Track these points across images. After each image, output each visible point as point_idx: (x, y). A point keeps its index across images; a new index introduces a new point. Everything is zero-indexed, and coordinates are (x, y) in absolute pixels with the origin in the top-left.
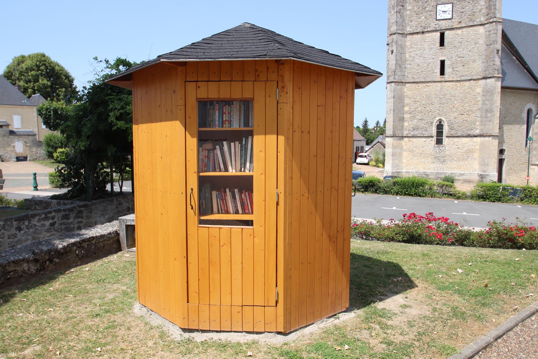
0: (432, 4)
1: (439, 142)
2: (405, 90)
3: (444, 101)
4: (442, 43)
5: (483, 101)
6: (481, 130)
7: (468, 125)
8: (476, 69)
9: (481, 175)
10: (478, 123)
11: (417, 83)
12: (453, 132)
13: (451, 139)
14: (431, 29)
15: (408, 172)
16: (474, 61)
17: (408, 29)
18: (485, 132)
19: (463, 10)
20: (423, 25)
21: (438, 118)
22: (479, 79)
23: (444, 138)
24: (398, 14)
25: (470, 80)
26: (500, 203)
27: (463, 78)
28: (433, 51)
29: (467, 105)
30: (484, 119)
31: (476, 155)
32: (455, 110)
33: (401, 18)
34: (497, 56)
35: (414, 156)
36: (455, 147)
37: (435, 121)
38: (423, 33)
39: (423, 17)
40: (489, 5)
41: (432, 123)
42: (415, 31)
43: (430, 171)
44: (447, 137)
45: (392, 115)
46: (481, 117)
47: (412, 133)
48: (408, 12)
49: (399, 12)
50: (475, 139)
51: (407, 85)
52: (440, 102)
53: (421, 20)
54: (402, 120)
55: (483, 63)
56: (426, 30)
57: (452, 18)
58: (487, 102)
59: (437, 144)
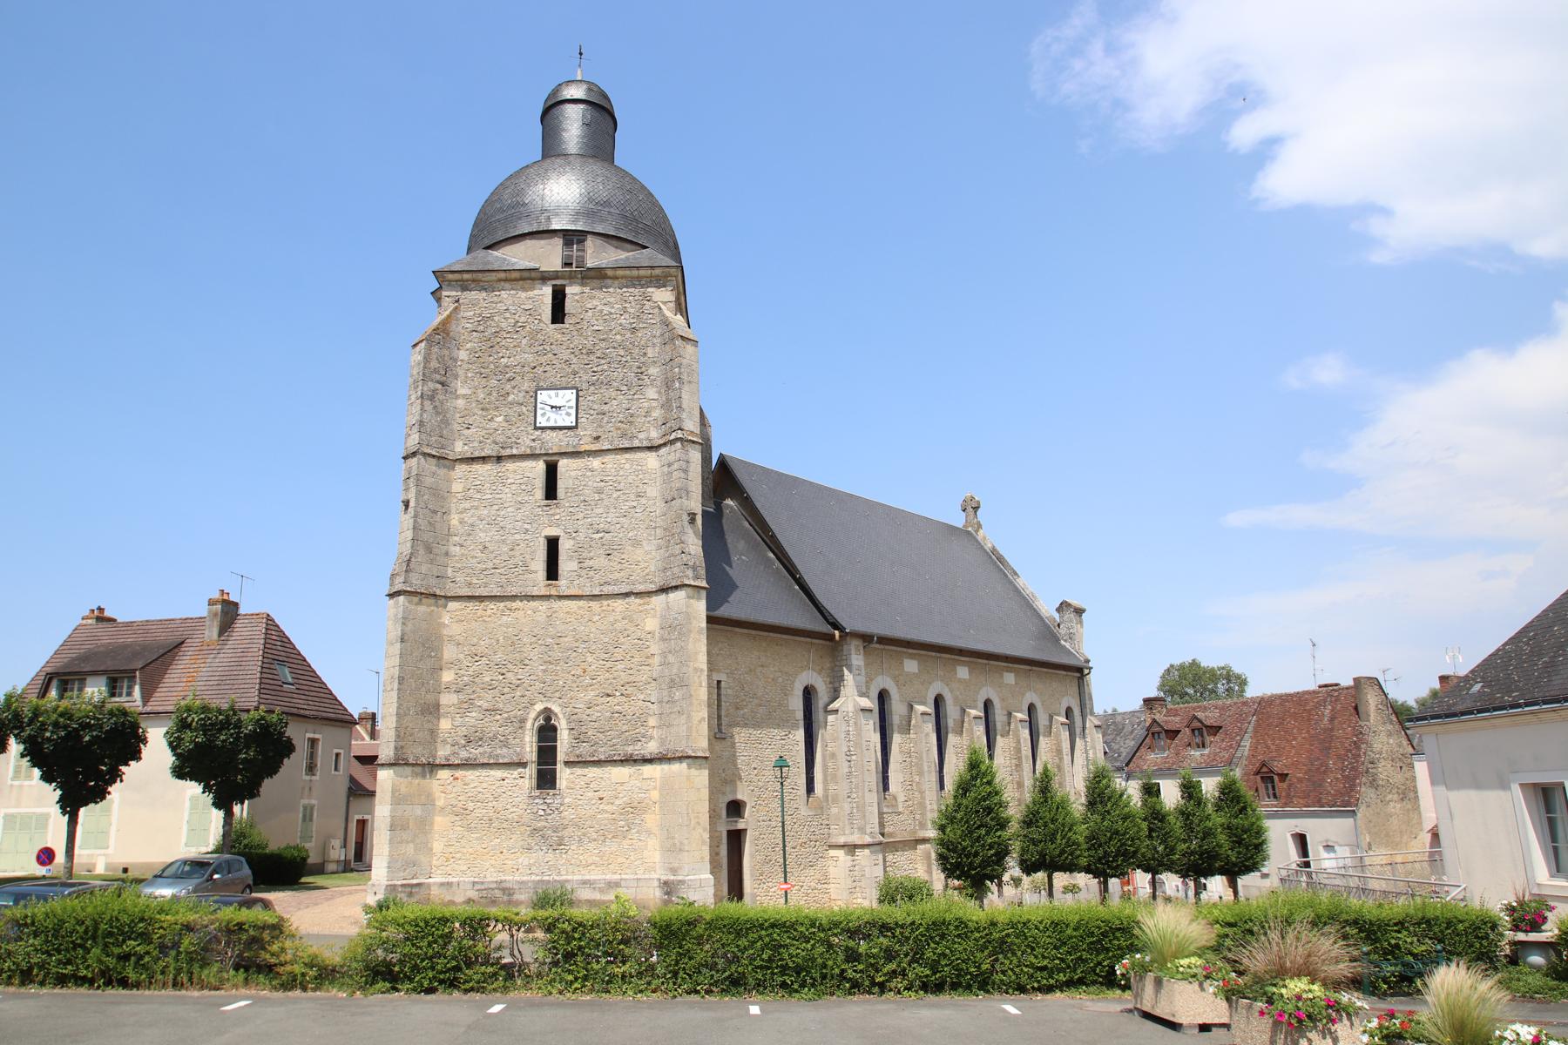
0: (526, 386)
1: (546, 780)
2: (446, 619)
3: (556, 654)
4: (551, 491)
5: (664, 654)
6: (662, 742)
7: (625, 728)
8: (642, 565)
9: (666, 883)
10: (652, 722)
11: (481, 598)
12: (584, 750)
13: (579, 771)
14: (522, 450)
15: (449, 884)
16: (637, 543)
17: (459, 448)
18: (671, 747)
19: (606, 408)
20: (501, 439)
21: (539, 707)
22: (649, 593)
23: (559, 767)
24: (427, 403)
25: (627, 595)
26: (456, 994)
27: (607, 589)
28: (526, 509)
29: (620, 666)
32: (588, 681)
33: (438, 413)
34: (689, 530)
35: (469, 829)
36: (590, 794)
37: (533, 715)
38: (499, 459)
39: (500, 419)
40: (669, 400)
41: (523, 721)
42: (477, 454)
43: (517, 878)
44: (567, 763)
45: (394, 694)
47: (464, 754)
48: (460, 403)
49: (432, 398)
50: (648, 770)
51: (452, 605)
52: (546, 658)
53: (495, 425)
54: (432, 710)
56: (508, 452)
57: (576, 427)
58: (671, 658)
59: (539, 787)
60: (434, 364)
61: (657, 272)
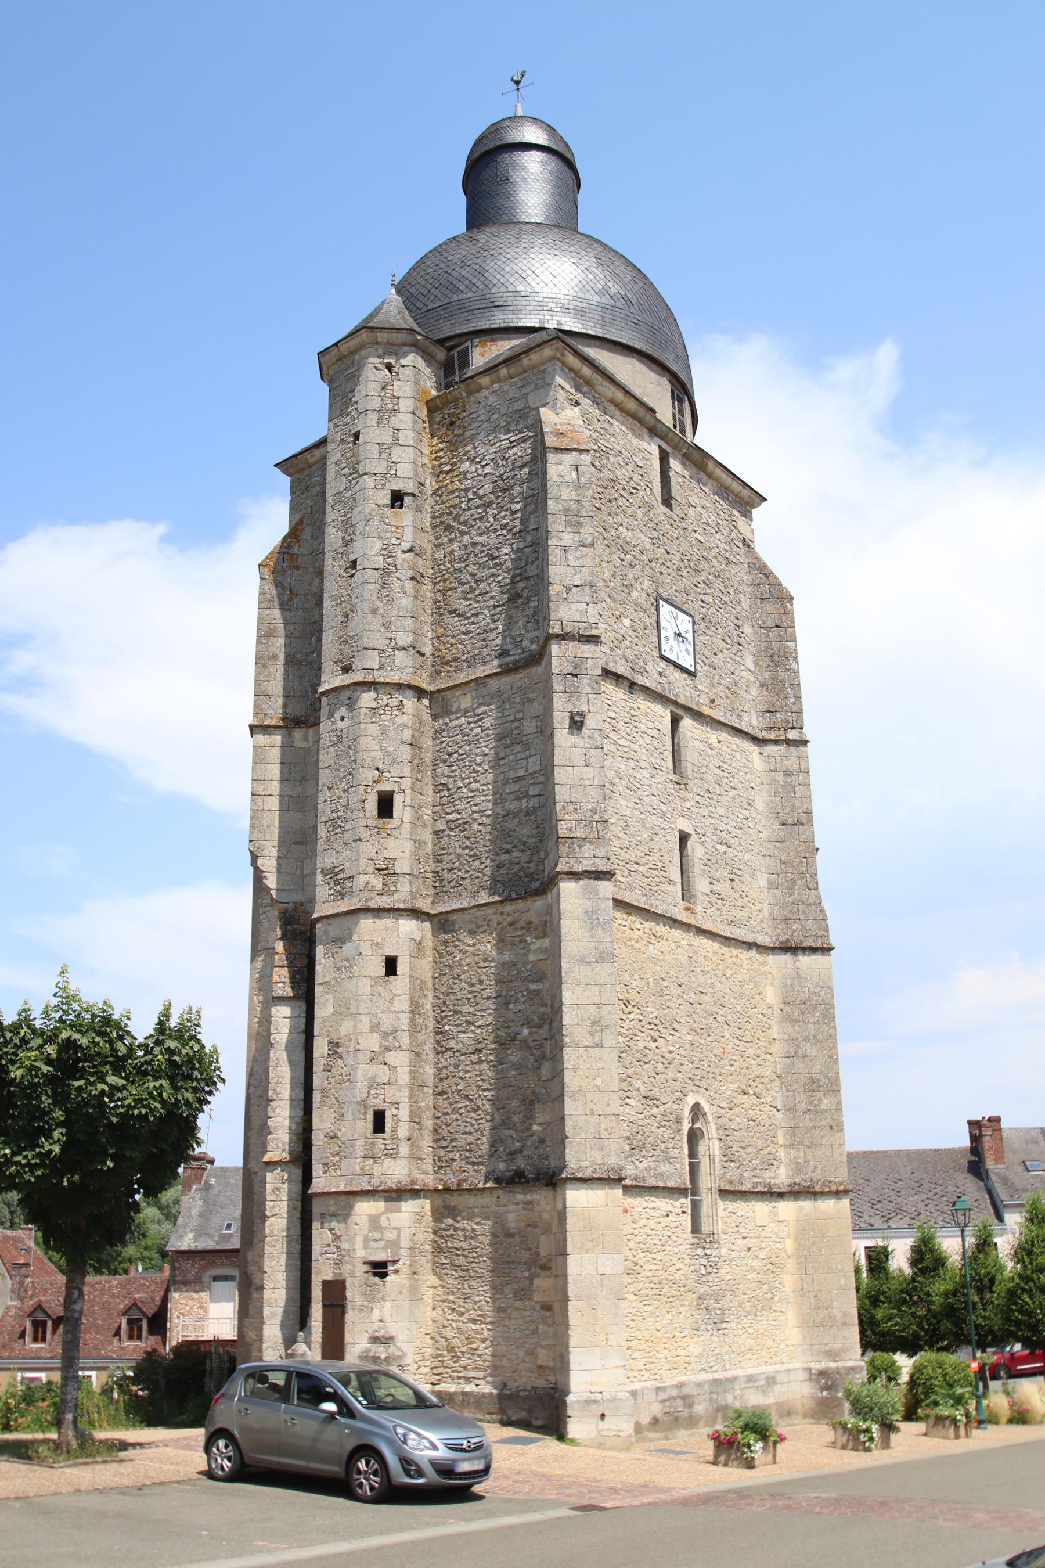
5: (792, 1041)
6: (798, 1168)
9: (822, 1373)
10: (781, 1140)
12: (733, 1173)
18: (817, 1175)
30: (807, 1121)
31: (788, 1281)
46: (792, 1110)
55: (772, 886)
58: (810, 1049)
61: (746, 493)
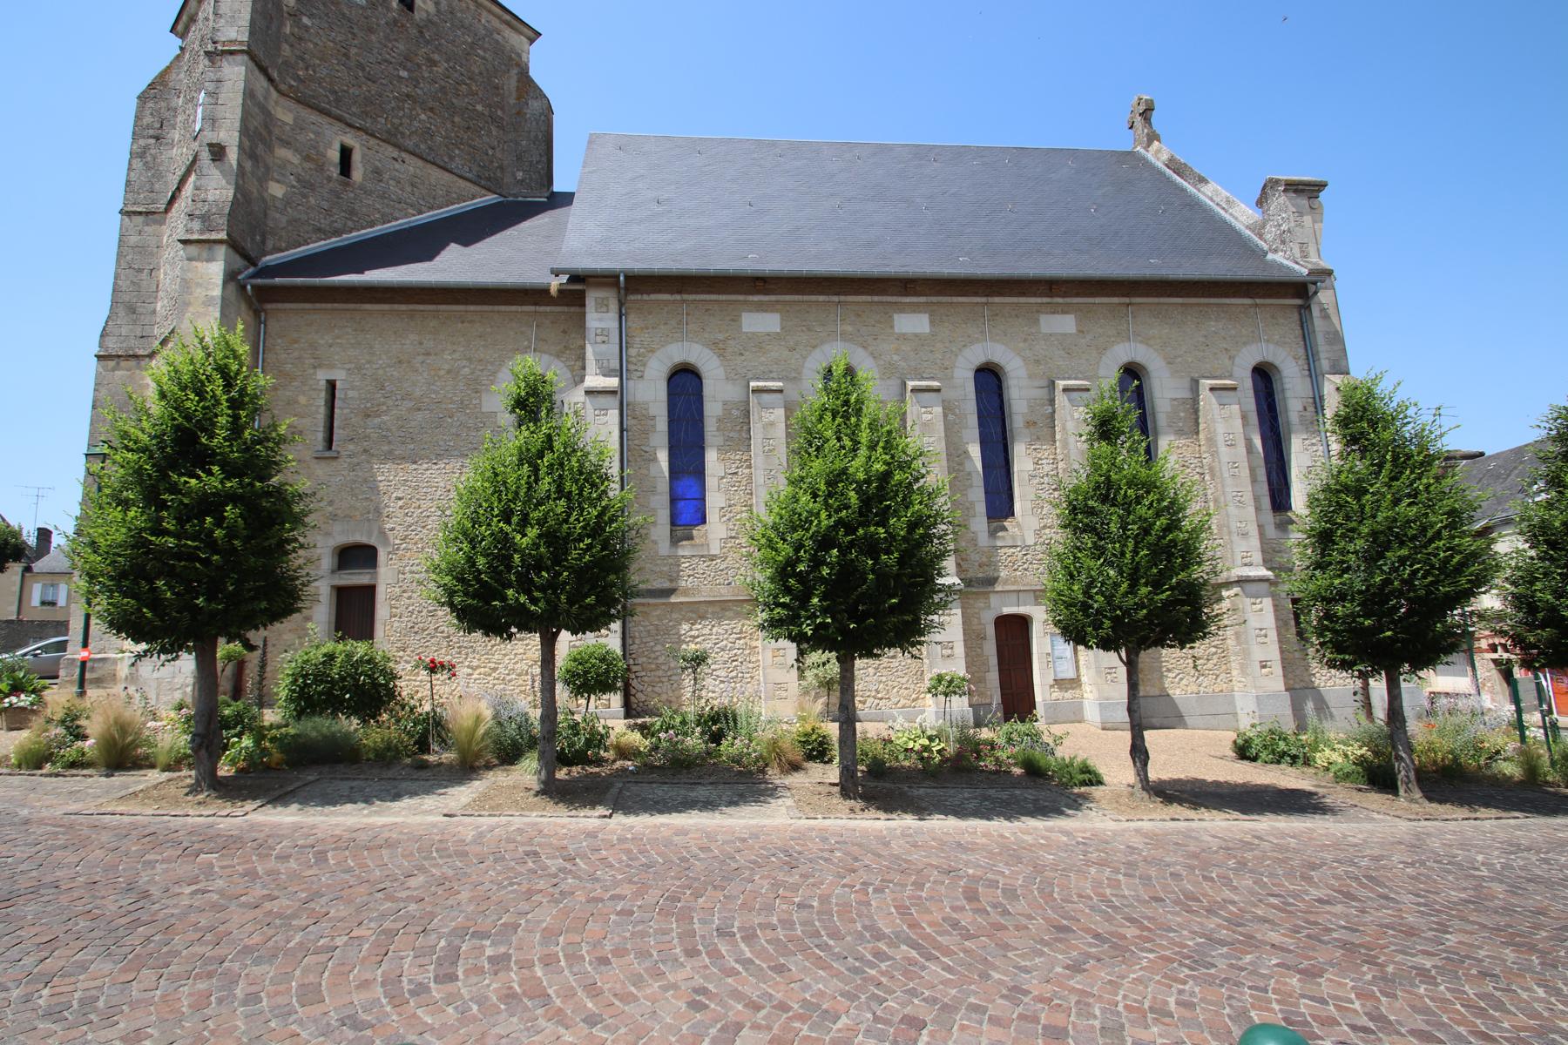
33: (149, 169)
60: (147, 120)
